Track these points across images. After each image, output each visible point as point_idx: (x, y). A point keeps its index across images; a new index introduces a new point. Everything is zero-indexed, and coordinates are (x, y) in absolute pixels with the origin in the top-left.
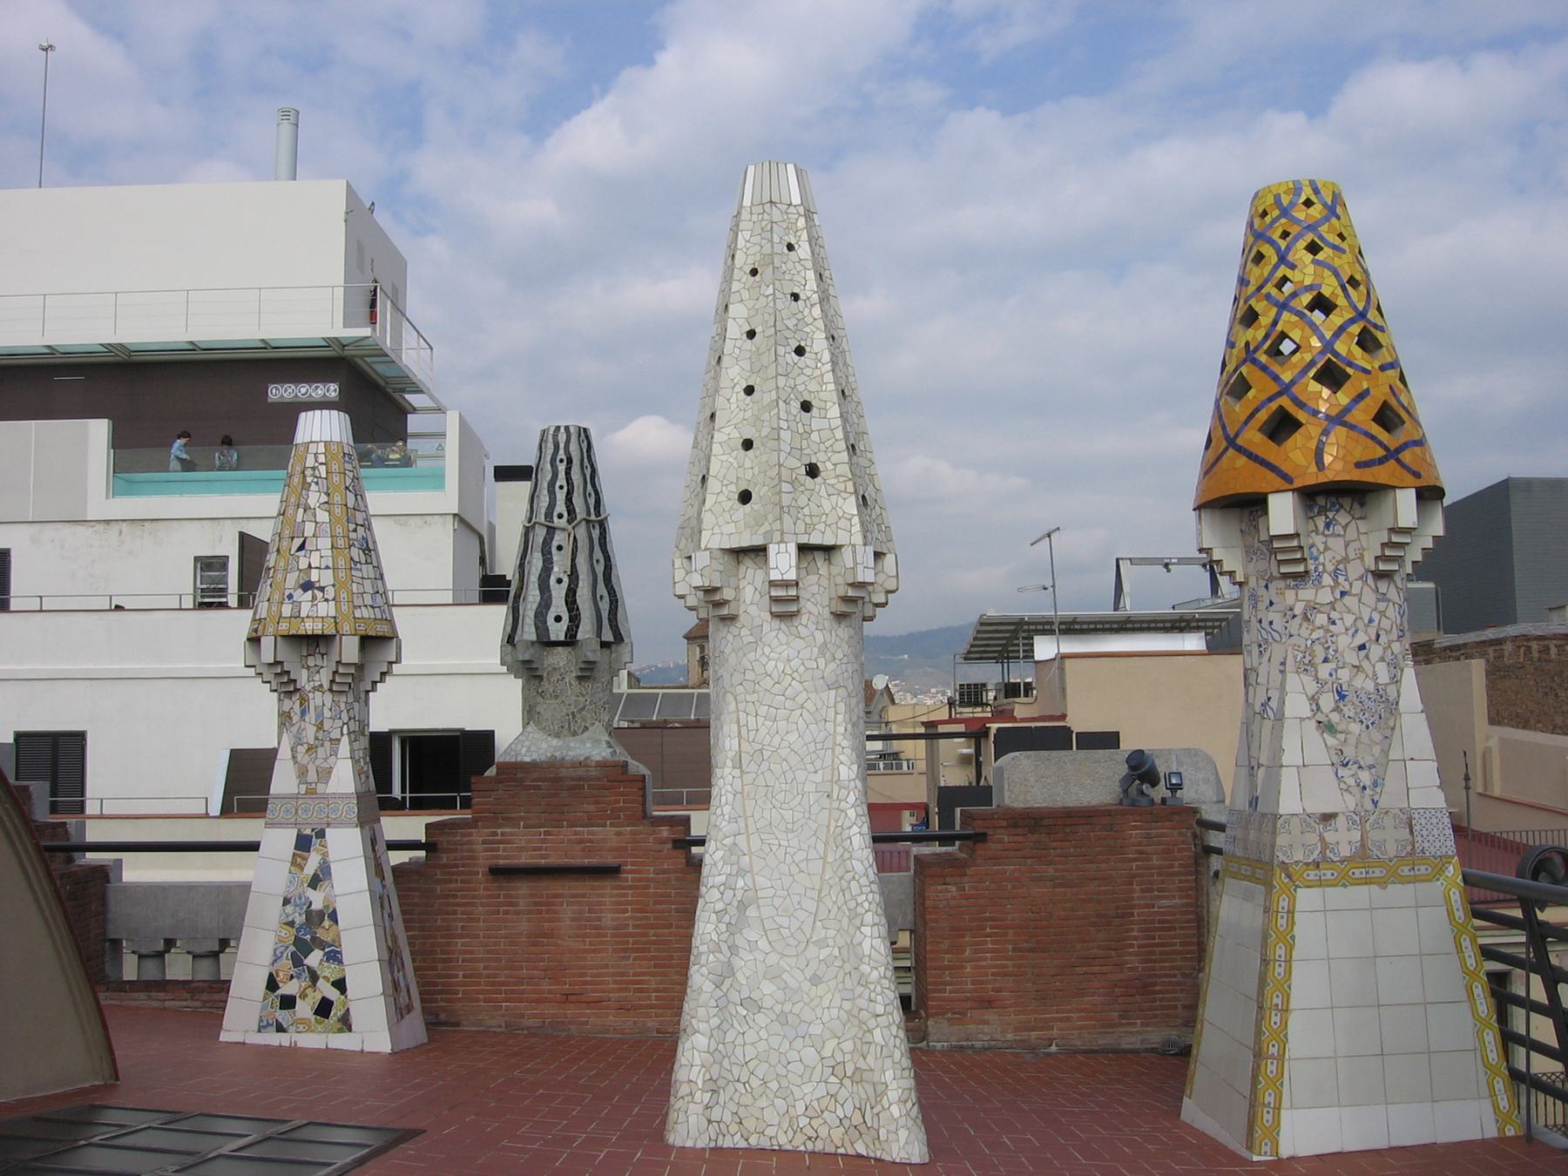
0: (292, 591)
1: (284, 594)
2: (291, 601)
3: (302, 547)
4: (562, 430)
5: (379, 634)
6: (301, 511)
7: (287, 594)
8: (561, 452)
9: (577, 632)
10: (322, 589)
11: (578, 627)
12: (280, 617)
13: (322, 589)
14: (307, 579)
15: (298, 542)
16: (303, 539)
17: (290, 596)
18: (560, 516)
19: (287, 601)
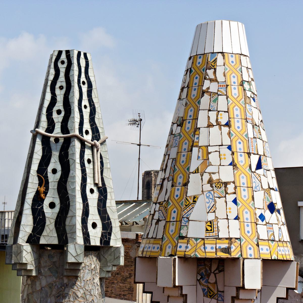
0: (262, 211)
1: (255, 214)
2: (264, 223)
3: (259, 166)
4: (82, 56)
5: (280, 258)
6: (250, 126)
7: (258, 215)
8: (83, 75)
9: (110, 239)
10: (279, 211)
11: (110, 234)
12: (258, 238)
13: (279, 211)
14: (270, 200)
15: (254, 160)
16: (258, 156)
17: (262, 217)
18: (87, 132)
19: (260, 222)
